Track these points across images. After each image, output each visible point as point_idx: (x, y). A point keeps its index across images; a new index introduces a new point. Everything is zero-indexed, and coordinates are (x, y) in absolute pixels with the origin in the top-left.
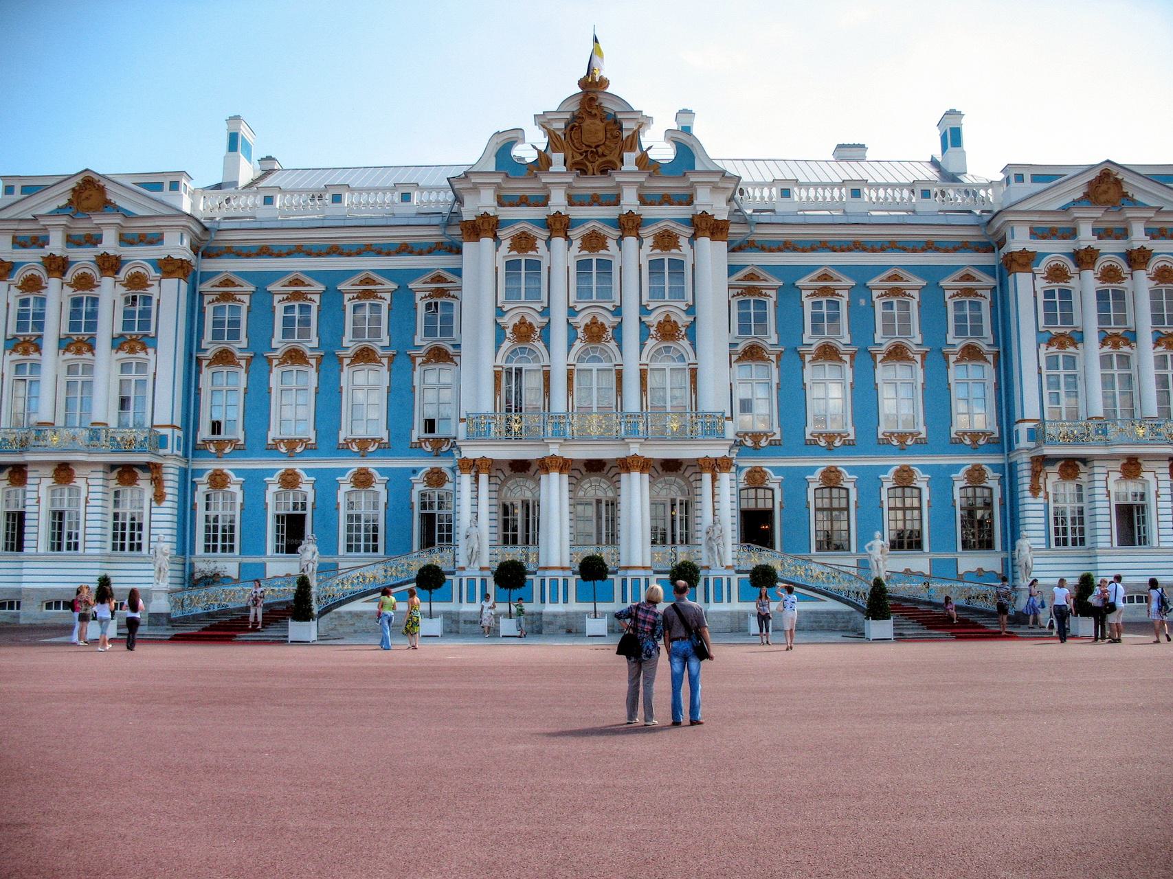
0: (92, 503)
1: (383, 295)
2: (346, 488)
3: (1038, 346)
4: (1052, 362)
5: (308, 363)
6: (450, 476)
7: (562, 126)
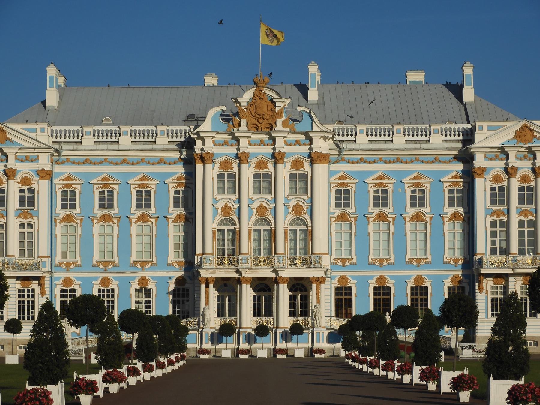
3: (486, 217)
4: (493, 224)
5: (113, 221)
6: (188, 280)
7: (245, 104)
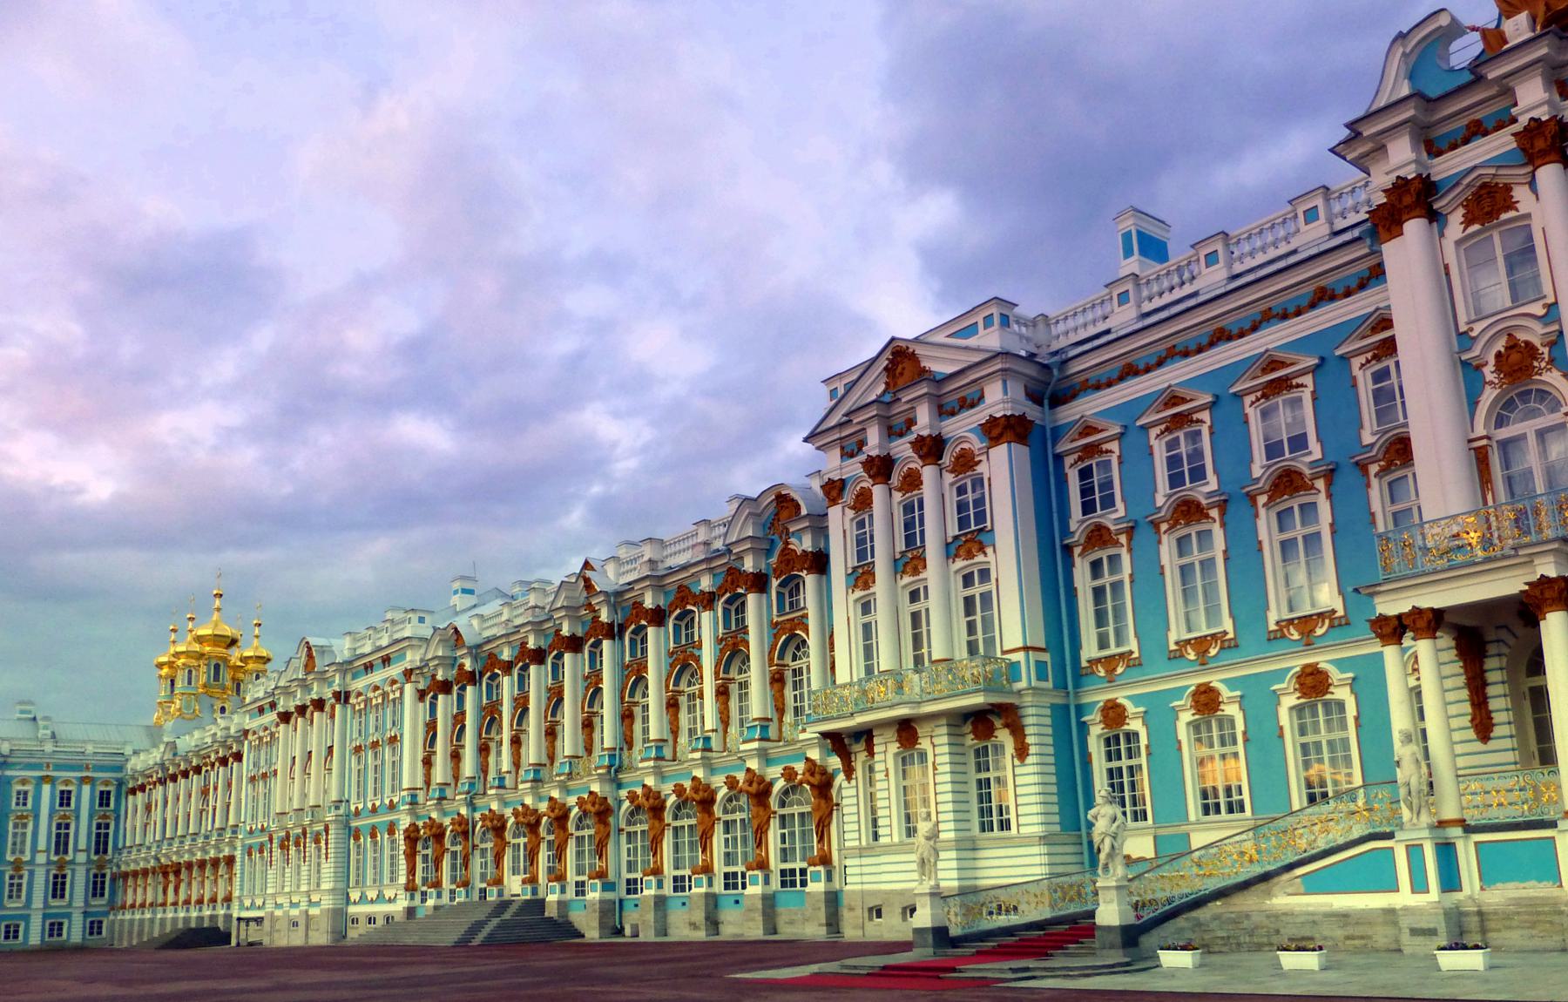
0: (941, 769)
1: (1299, 380)
2: (1290, 700)
5: (1207, 516)
